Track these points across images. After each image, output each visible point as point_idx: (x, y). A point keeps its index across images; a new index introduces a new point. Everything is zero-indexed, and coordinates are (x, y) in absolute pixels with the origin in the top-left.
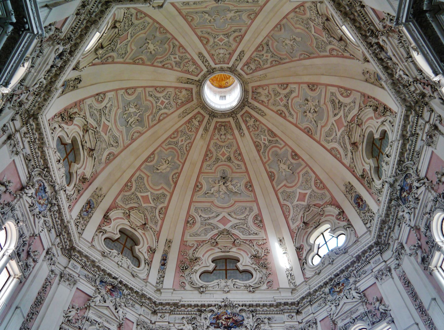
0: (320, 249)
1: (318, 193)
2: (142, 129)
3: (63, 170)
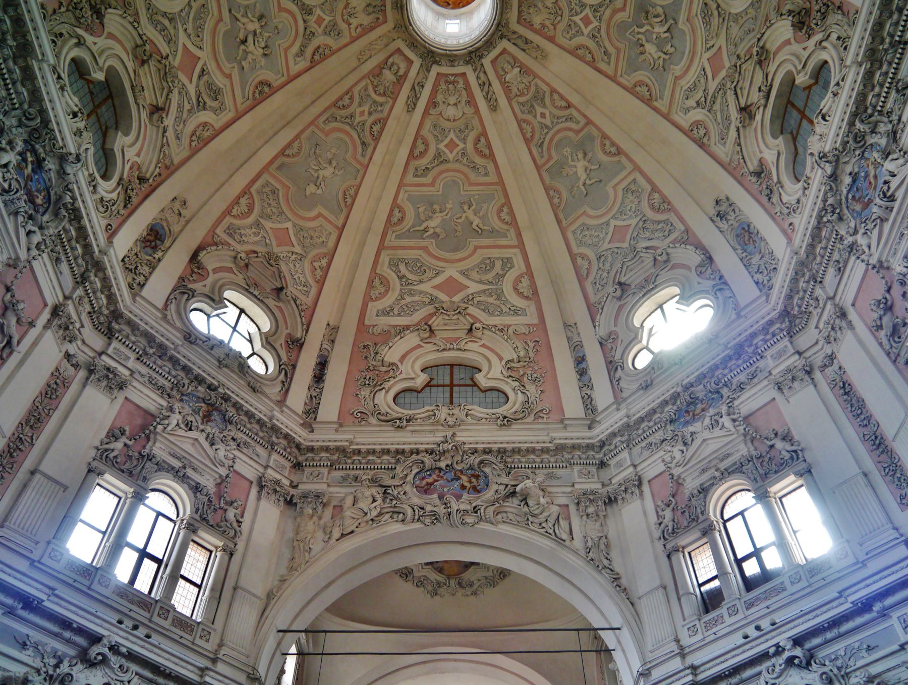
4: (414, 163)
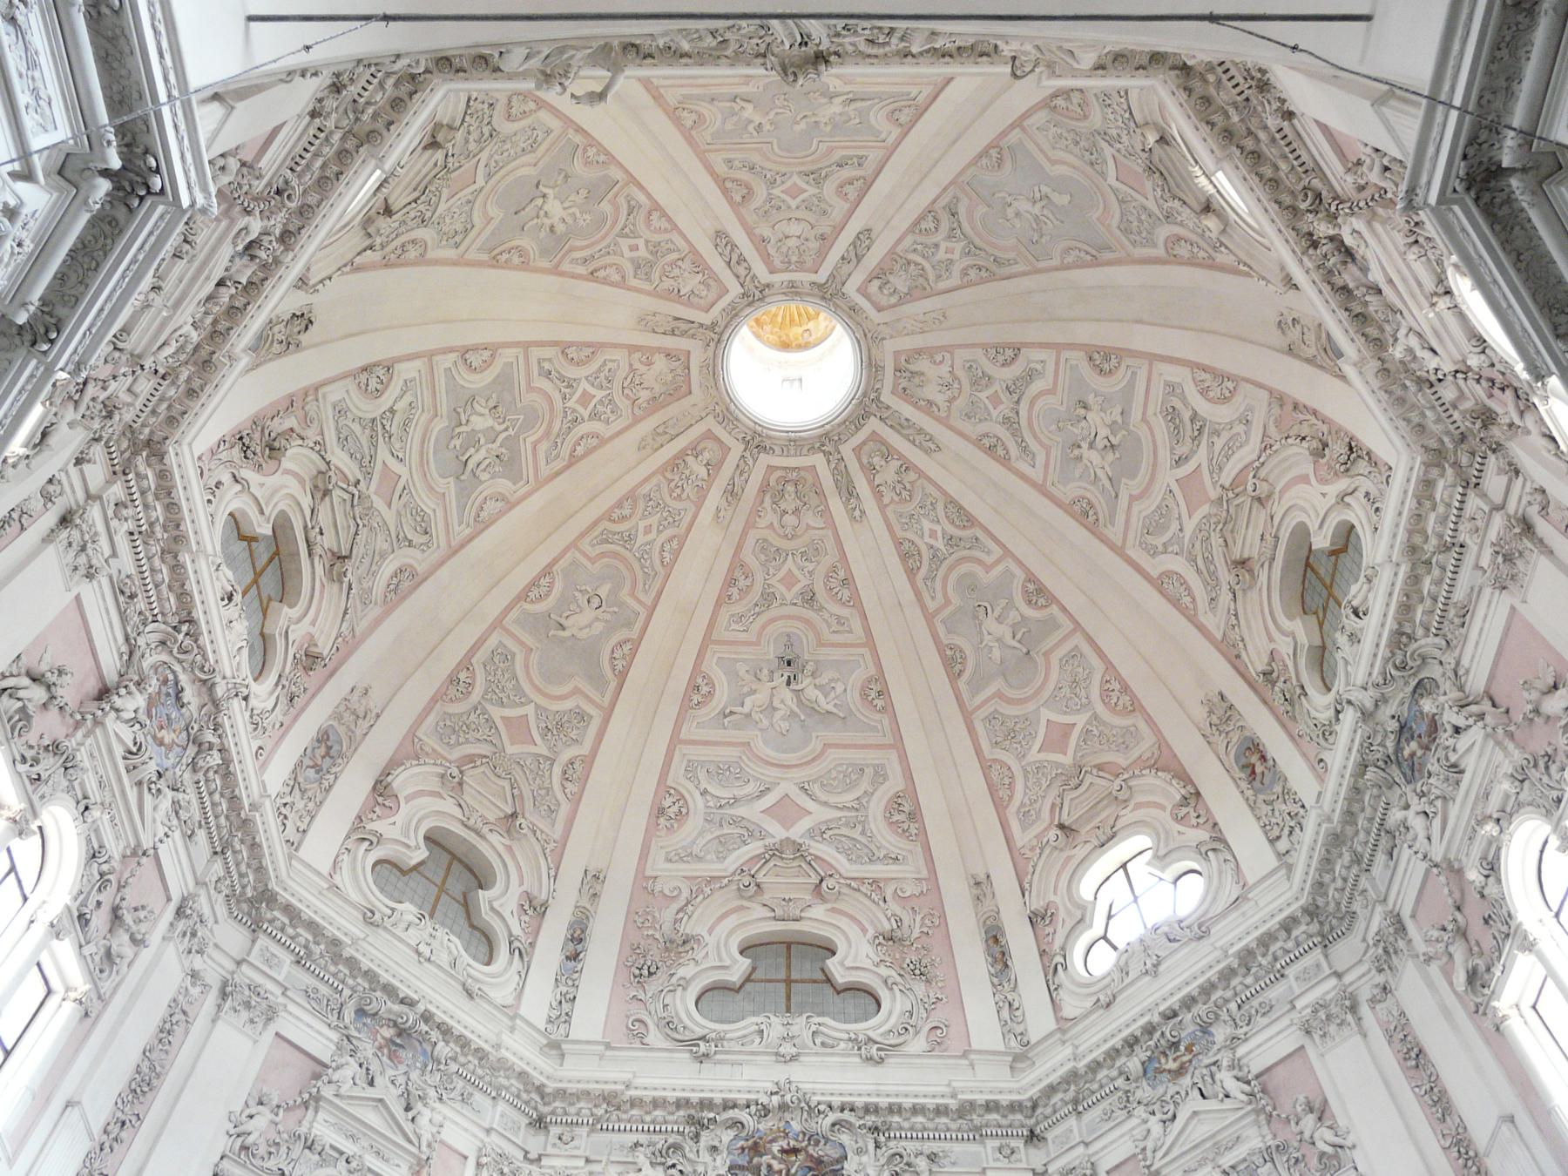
0: (1111, 922)
1: (1113, 727)
2: (514, 488)
3: (241, 627)
4: (867, 170)
